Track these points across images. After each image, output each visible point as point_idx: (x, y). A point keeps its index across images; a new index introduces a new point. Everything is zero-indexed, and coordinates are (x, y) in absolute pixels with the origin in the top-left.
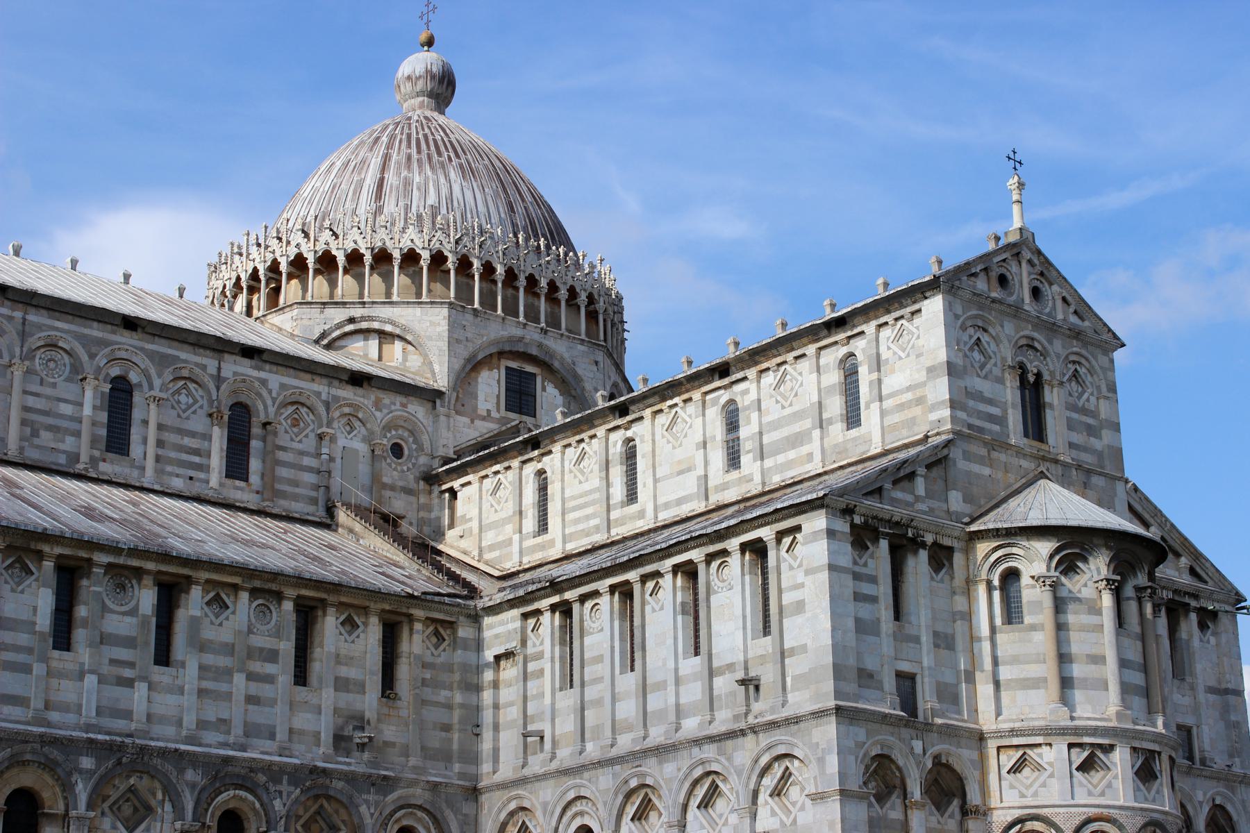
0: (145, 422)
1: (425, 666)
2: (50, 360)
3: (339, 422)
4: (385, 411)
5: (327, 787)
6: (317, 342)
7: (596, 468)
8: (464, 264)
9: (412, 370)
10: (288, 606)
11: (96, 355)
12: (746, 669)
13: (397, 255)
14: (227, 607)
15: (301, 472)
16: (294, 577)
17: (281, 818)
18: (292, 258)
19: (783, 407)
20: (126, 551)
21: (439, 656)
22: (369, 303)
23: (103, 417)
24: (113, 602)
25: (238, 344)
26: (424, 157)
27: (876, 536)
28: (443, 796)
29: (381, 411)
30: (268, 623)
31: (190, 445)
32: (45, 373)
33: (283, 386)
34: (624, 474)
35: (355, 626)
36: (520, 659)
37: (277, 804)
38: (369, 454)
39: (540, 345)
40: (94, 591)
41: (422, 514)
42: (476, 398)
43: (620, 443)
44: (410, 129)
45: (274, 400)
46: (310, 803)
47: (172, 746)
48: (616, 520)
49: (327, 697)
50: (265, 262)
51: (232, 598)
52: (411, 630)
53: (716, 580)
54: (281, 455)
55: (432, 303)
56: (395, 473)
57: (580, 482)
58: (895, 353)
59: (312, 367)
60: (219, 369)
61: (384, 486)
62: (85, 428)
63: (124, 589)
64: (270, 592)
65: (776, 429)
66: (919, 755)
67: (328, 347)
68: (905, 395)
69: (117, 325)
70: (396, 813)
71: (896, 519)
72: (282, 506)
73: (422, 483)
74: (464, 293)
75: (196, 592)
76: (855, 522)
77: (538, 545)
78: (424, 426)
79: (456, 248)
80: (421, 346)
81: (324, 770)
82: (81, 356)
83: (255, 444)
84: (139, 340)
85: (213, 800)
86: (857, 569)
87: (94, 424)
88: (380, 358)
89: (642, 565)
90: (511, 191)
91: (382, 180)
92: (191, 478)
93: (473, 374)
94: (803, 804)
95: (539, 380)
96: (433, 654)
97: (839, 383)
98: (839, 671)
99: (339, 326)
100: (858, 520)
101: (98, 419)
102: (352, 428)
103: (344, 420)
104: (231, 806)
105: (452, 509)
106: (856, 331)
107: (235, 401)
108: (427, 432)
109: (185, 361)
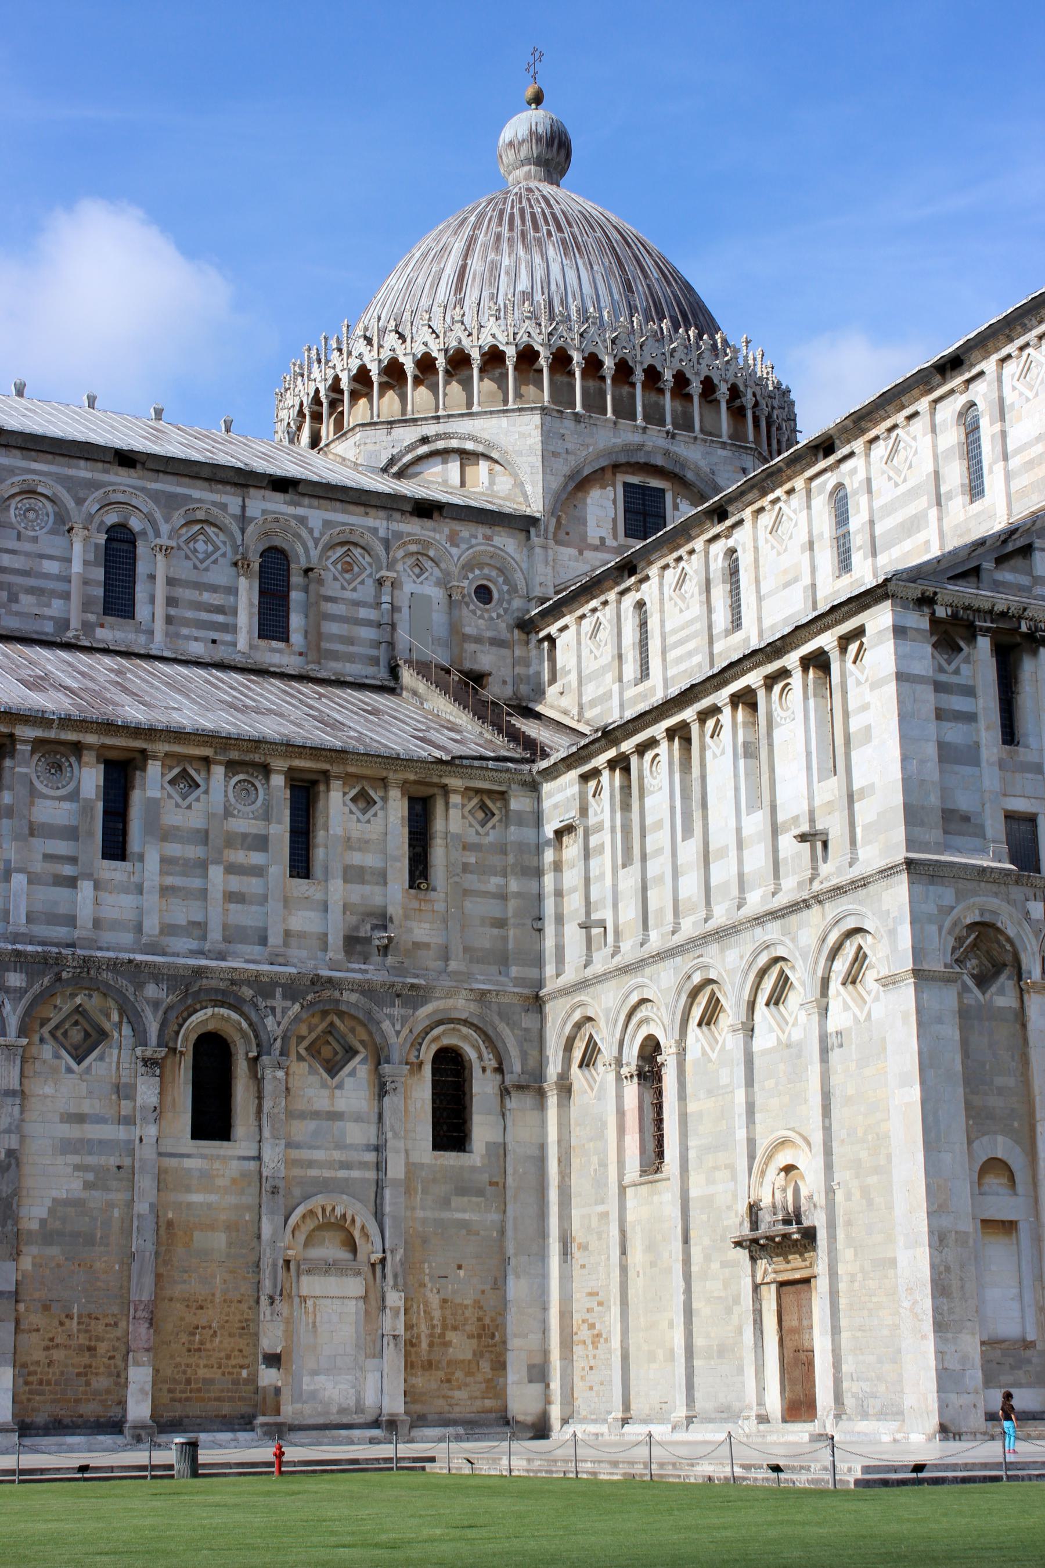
0: (152, 577)
1: (466, 847)
2: (28, 510)
3: (404, 563)
4: (464, 546)
5: (337, 1001)
6: (385, 470)
7: (696, 590)
8: (561, 360)
9: (501, 494)
10: (278, 780)
11: (85, 500)
12: (812, 820)
13: (475, 355)
14: (198, 786)
16: (282, 744)
17: (275, 1040)
18: (355, 372)
19: (896, 485)
20: (57, 722)
21: (487, 834)
22: (444, 417)
23: (99, 573)
24: (46, 786)
25: (263, 475)
26: (517, 234)
27: (972, 633)
28: (494, 1007)
29: (458, 546)
30: (253, 803)
31: (211, 601)
32: (23, 525)
33: (327, 524)
34: (728, 595)
35: (370, 802)
36: (580, 831)
37: (270, 1022)
38: (444, 601)
39: (667, 453)
40: (19, 773)
41: (518, 670)
42: (585, 523)
43: (721, 555)
44: (504, 204)
45: (316, 541)
46: (315, 1020)
47: (125, 956)
49: (337, 890)
50: (326, 380)
51: (203, 774)
52: (447, 804)
53: (779, 708)
54: (330, 608)
55: (520, 410)
56: (481, 621)
57: (681, 611)
58: (1021, 394)
59: (363, 498)
60: (244, 507)
61: (466, 638)
62: (75, 588)
64: (253, 764)
65: (889, 515)
66: (1038, 921)
67: (400, 475)
68: (1034, 448)
70: (432, 1029)
71: (1000, 607)
72: (331, 669)
73: (516, 631)
74: (562, 395)
75: (154, 768)
76: (937, 614)
77: (639, 694)
78: (516, 563)
79: (549, 340)
80: (510, 464)
81: (330, 980)
82: (65, 501)
83: (295, 596)
84: (139, 478)
85: (185, 1020)
86: (943, 678)
87: (86, 582)
88: (463, 484)
89: (697, 699)
90: (631, 268)
91: (464, 267)
92: (214, 642)
93: (580, 495)
94: (878, 992)
96: (478, 833)
97: (959, 443)
98: (912, 814)
99: (411, 448)
100: (941, 612)
101: (92, 576)
102: (423, 570)
103: (411, 561)
104: (210, 1027)
105: (552, 660)
106: (975, 371)
107: (267, 546)
108: (521, 570)
109: (200, 501)
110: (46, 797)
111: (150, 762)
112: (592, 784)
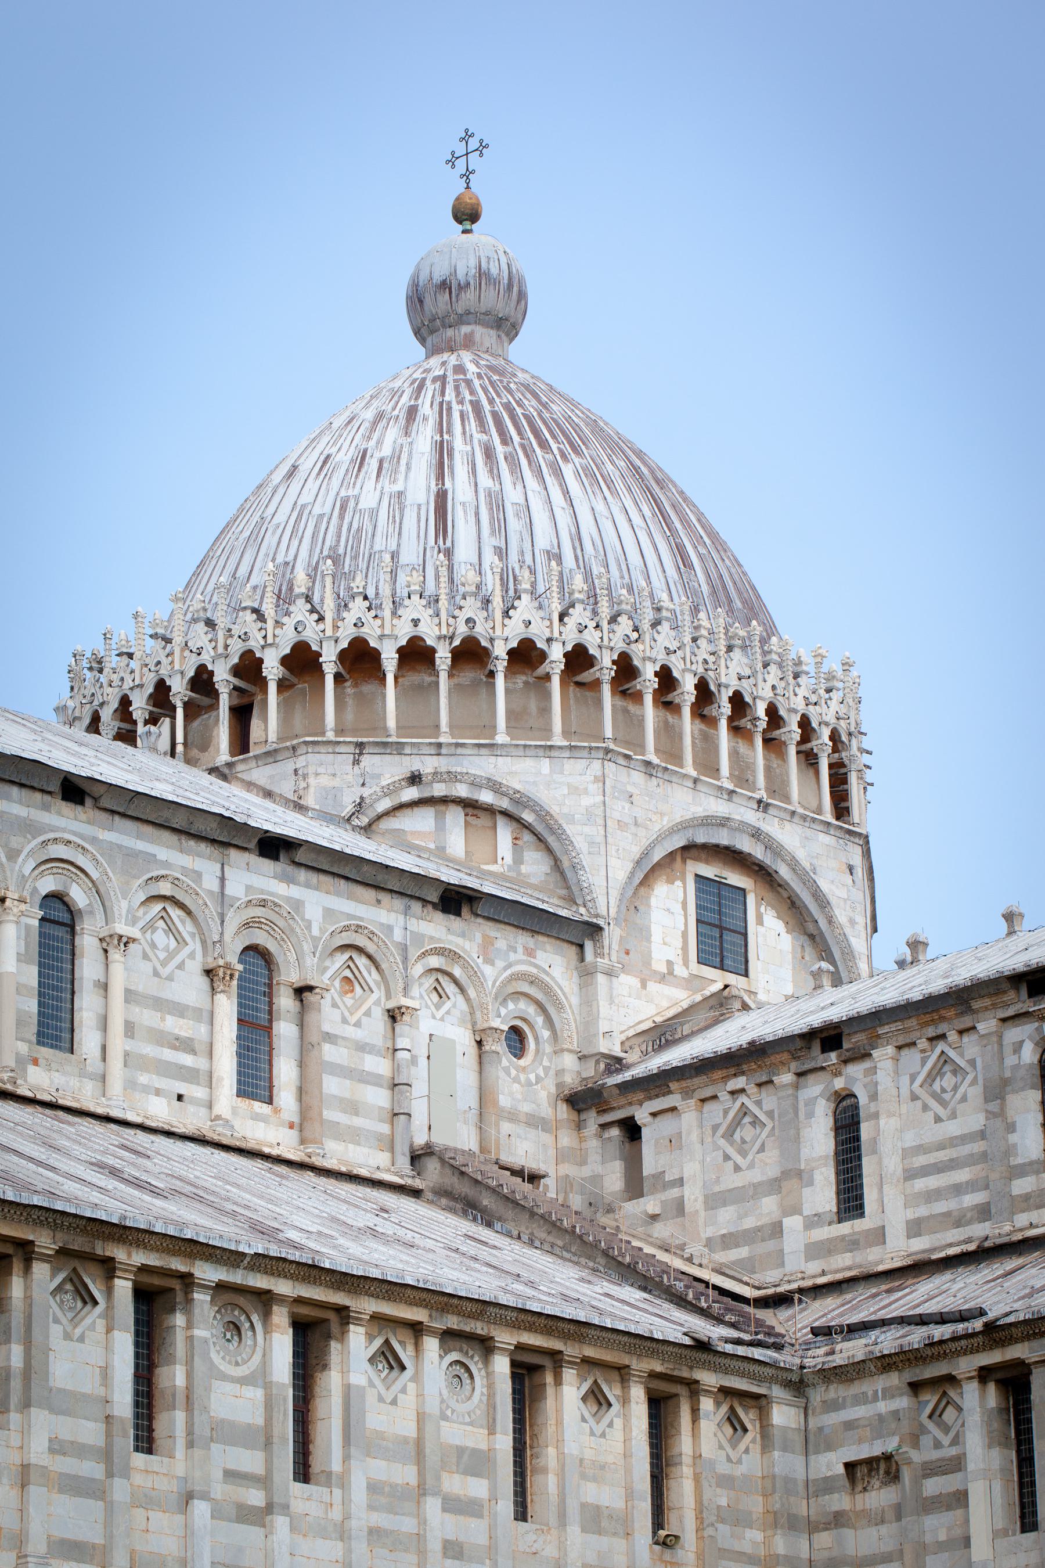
0: (104, 987)
3: (421, 985)
4: (500, 964)
10: (502, 1365)
11: (19, 852)
14: (403, 1368)
15: (363, 1085)
20: (248, 1259)
21: (739, 1461)
24: (223, 1358)
29: (493, 964)
30: (469, 1398)
31: (176, 1031)
33: (328, 913)
38: (472, 1050)
39: (756, 834)
42: (648, 939)
48: (1027, 1197)
52: (695, 1411)
56: (516, 1085)
57: (938, 1119)
59: (380, 877)
63: (238, 1329)
67: (367, 830)
69: (50, 793)
77: (843, 1238)
78: (564, 994)
83: (285, 1030)
84: (89, 823)
91: (441, 500)
92: (180, 1097)
93: (642, 890)
95: (751, 900)
101: (23, 980)
107: (247, 943)
109: (166, 864)
110: (224, 1377)
111: (352, 1327)
112: (930, 1399)
